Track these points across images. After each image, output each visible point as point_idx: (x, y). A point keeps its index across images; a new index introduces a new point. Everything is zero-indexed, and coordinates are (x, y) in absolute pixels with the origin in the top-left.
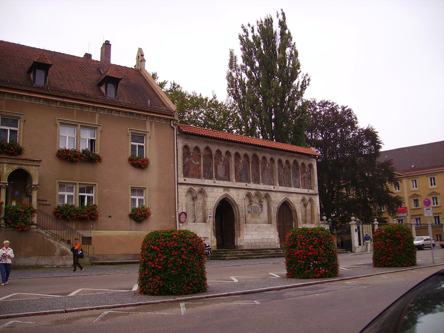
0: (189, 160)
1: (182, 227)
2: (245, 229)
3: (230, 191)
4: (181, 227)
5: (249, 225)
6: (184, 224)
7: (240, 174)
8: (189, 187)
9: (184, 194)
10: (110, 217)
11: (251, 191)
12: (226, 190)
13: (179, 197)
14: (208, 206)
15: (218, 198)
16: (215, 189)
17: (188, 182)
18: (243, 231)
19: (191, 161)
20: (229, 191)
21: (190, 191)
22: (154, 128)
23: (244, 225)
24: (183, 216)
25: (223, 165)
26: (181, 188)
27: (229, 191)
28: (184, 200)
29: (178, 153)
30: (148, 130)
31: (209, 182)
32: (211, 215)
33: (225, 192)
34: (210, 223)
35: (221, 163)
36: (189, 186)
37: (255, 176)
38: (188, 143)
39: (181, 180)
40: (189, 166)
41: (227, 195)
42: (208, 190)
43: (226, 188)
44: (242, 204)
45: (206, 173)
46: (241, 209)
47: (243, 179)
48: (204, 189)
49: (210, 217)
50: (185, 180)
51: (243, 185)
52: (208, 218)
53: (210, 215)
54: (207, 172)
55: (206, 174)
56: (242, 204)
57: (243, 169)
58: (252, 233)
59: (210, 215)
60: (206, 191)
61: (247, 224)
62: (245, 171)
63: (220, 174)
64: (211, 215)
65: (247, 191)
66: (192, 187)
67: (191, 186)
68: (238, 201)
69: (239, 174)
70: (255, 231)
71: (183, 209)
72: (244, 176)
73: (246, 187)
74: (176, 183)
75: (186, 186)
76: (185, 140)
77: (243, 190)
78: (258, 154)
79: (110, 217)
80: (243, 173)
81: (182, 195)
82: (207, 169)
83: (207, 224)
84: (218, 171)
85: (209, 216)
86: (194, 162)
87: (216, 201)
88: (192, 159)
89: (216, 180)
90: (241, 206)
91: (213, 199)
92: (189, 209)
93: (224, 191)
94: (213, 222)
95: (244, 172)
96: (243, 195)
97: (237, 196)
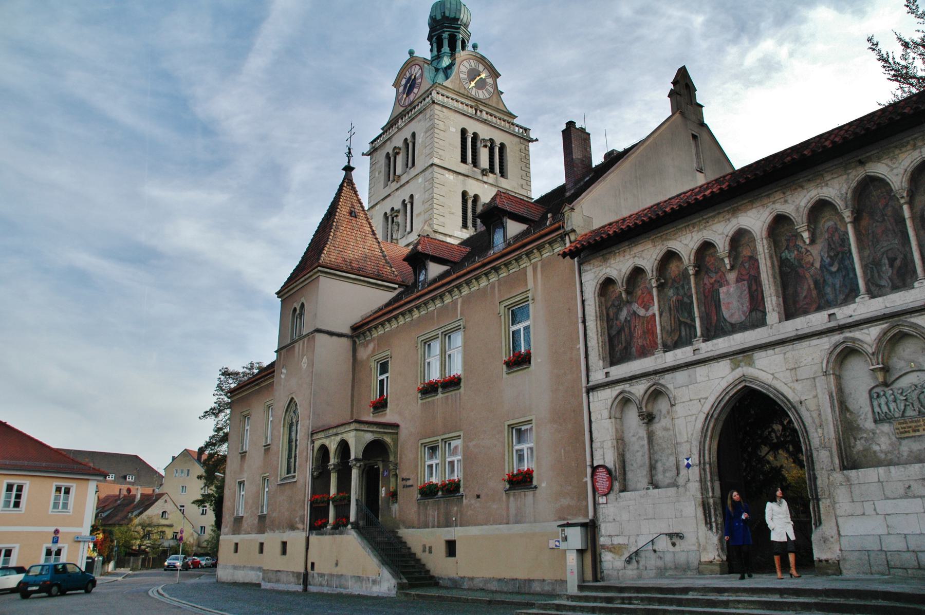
0: (628, 312)
1: (605, 506)
2: (841, 495)
3: (757, 362)
4: (602, 506)
5: (869, 475)
6: (612, 496)
7: (816, 283)
8: (618, 389)
9: (606, 414)
10: (478, 497)
11: (857, 334)
12: (742, 364)
13: (593, 425)
14: (680, 433)
15: (711, 400)
16: (700, 371)
17: (614, 378)
18: (834, 503)
19: (635, 313)
20: (751, 364)
21: (625, 401)
22: (539, 275)
23: (838, 476)
24: (602, 475)
25: (738, 280)
26: (596, 399)
27: (751, 364)
28: (608, 429)
29: (587, 308)
30: (530, 284)
31: (678, 357)
32: (695, 460)
33: (738, 373)
34: (690, 485)
35: (732, 276)
36: (616, 388)
37: (898, 263)
38: (608, 270)
39: (598, 376)
40: (630, 329)
41: (743, 378)
42: (668, 380)
43: (740, 357)
44: (816, 396)
45: (683, 329)
46: (815, 415)
47: (831, 296)
48: (662, 381)
49: (688, 466)
50: (607, 374)
51: (817, 320)
52: (683, 472)
53: (688, 459)
54: (685, 324)
55: (683, 333)
56: (816, 396)
57: (827, 260)
58: (885, 506)
59: (688, 459)
60: (670, 386)
61: (853, 473)
62: (842, 261)
63: (732, 315)
64: (690, 461)
65: (837, 338)
66: (626, 387)
67: (623, 386)
68: (794, 390)
69: (812, 286)
70: (906, 496)
71: (605, 455)
72: (838, 282)
73: (833, 324)
74: (584, 390)
75: (609, 390)
76: (601, 268)
77: (815, 342)
78: (880, 169)
79: (478, 497)
80: (831, 273)
81: (599, 417)
82: (686, 315)
83: (681, 490)
84: (723, 307)
85: (686, 462)
86: (642, 312)
87: (707, 408)
88: (635, 307)
89: (704, 341)
90: (812, 404)
91: (695, 407)
92: (638, 451)
93: (733, 370)
94: (702, 481)
95: (834, 269)
96: (818, 360)
97: (788, 373)
